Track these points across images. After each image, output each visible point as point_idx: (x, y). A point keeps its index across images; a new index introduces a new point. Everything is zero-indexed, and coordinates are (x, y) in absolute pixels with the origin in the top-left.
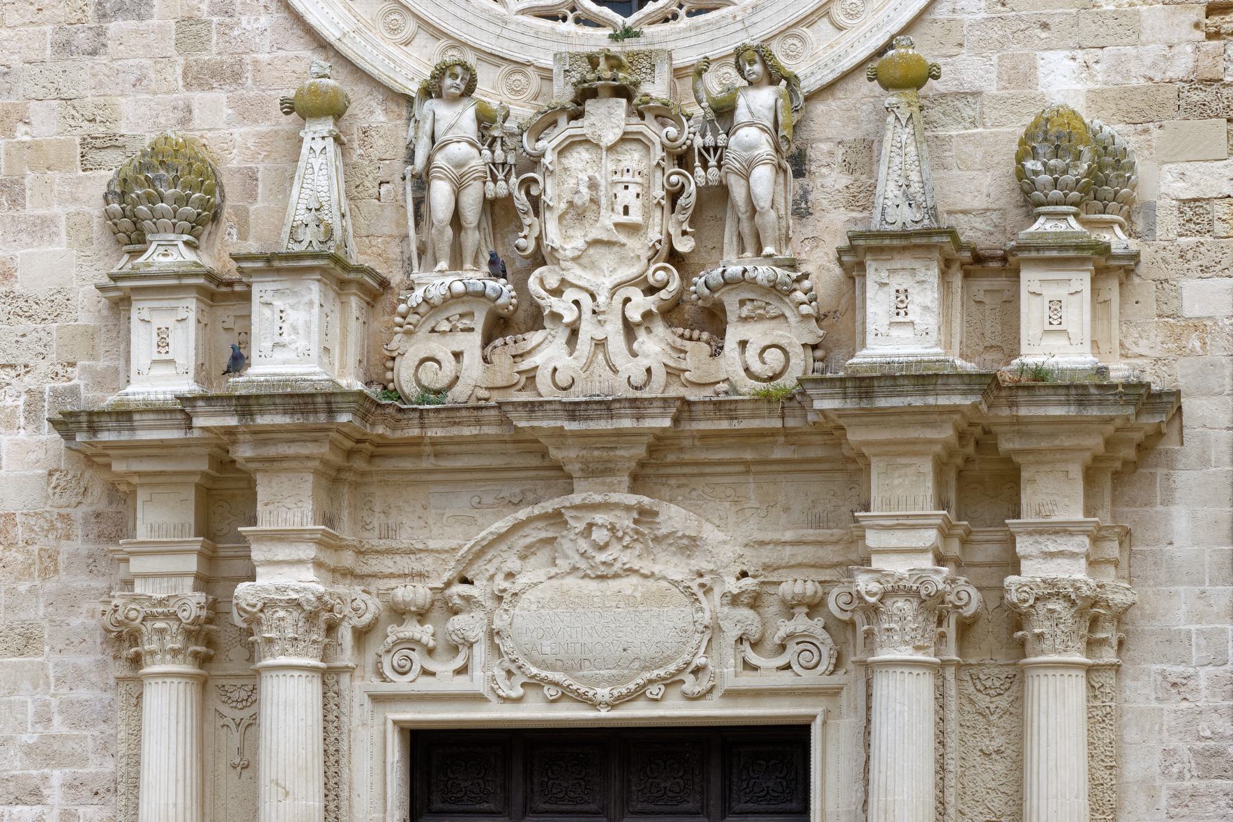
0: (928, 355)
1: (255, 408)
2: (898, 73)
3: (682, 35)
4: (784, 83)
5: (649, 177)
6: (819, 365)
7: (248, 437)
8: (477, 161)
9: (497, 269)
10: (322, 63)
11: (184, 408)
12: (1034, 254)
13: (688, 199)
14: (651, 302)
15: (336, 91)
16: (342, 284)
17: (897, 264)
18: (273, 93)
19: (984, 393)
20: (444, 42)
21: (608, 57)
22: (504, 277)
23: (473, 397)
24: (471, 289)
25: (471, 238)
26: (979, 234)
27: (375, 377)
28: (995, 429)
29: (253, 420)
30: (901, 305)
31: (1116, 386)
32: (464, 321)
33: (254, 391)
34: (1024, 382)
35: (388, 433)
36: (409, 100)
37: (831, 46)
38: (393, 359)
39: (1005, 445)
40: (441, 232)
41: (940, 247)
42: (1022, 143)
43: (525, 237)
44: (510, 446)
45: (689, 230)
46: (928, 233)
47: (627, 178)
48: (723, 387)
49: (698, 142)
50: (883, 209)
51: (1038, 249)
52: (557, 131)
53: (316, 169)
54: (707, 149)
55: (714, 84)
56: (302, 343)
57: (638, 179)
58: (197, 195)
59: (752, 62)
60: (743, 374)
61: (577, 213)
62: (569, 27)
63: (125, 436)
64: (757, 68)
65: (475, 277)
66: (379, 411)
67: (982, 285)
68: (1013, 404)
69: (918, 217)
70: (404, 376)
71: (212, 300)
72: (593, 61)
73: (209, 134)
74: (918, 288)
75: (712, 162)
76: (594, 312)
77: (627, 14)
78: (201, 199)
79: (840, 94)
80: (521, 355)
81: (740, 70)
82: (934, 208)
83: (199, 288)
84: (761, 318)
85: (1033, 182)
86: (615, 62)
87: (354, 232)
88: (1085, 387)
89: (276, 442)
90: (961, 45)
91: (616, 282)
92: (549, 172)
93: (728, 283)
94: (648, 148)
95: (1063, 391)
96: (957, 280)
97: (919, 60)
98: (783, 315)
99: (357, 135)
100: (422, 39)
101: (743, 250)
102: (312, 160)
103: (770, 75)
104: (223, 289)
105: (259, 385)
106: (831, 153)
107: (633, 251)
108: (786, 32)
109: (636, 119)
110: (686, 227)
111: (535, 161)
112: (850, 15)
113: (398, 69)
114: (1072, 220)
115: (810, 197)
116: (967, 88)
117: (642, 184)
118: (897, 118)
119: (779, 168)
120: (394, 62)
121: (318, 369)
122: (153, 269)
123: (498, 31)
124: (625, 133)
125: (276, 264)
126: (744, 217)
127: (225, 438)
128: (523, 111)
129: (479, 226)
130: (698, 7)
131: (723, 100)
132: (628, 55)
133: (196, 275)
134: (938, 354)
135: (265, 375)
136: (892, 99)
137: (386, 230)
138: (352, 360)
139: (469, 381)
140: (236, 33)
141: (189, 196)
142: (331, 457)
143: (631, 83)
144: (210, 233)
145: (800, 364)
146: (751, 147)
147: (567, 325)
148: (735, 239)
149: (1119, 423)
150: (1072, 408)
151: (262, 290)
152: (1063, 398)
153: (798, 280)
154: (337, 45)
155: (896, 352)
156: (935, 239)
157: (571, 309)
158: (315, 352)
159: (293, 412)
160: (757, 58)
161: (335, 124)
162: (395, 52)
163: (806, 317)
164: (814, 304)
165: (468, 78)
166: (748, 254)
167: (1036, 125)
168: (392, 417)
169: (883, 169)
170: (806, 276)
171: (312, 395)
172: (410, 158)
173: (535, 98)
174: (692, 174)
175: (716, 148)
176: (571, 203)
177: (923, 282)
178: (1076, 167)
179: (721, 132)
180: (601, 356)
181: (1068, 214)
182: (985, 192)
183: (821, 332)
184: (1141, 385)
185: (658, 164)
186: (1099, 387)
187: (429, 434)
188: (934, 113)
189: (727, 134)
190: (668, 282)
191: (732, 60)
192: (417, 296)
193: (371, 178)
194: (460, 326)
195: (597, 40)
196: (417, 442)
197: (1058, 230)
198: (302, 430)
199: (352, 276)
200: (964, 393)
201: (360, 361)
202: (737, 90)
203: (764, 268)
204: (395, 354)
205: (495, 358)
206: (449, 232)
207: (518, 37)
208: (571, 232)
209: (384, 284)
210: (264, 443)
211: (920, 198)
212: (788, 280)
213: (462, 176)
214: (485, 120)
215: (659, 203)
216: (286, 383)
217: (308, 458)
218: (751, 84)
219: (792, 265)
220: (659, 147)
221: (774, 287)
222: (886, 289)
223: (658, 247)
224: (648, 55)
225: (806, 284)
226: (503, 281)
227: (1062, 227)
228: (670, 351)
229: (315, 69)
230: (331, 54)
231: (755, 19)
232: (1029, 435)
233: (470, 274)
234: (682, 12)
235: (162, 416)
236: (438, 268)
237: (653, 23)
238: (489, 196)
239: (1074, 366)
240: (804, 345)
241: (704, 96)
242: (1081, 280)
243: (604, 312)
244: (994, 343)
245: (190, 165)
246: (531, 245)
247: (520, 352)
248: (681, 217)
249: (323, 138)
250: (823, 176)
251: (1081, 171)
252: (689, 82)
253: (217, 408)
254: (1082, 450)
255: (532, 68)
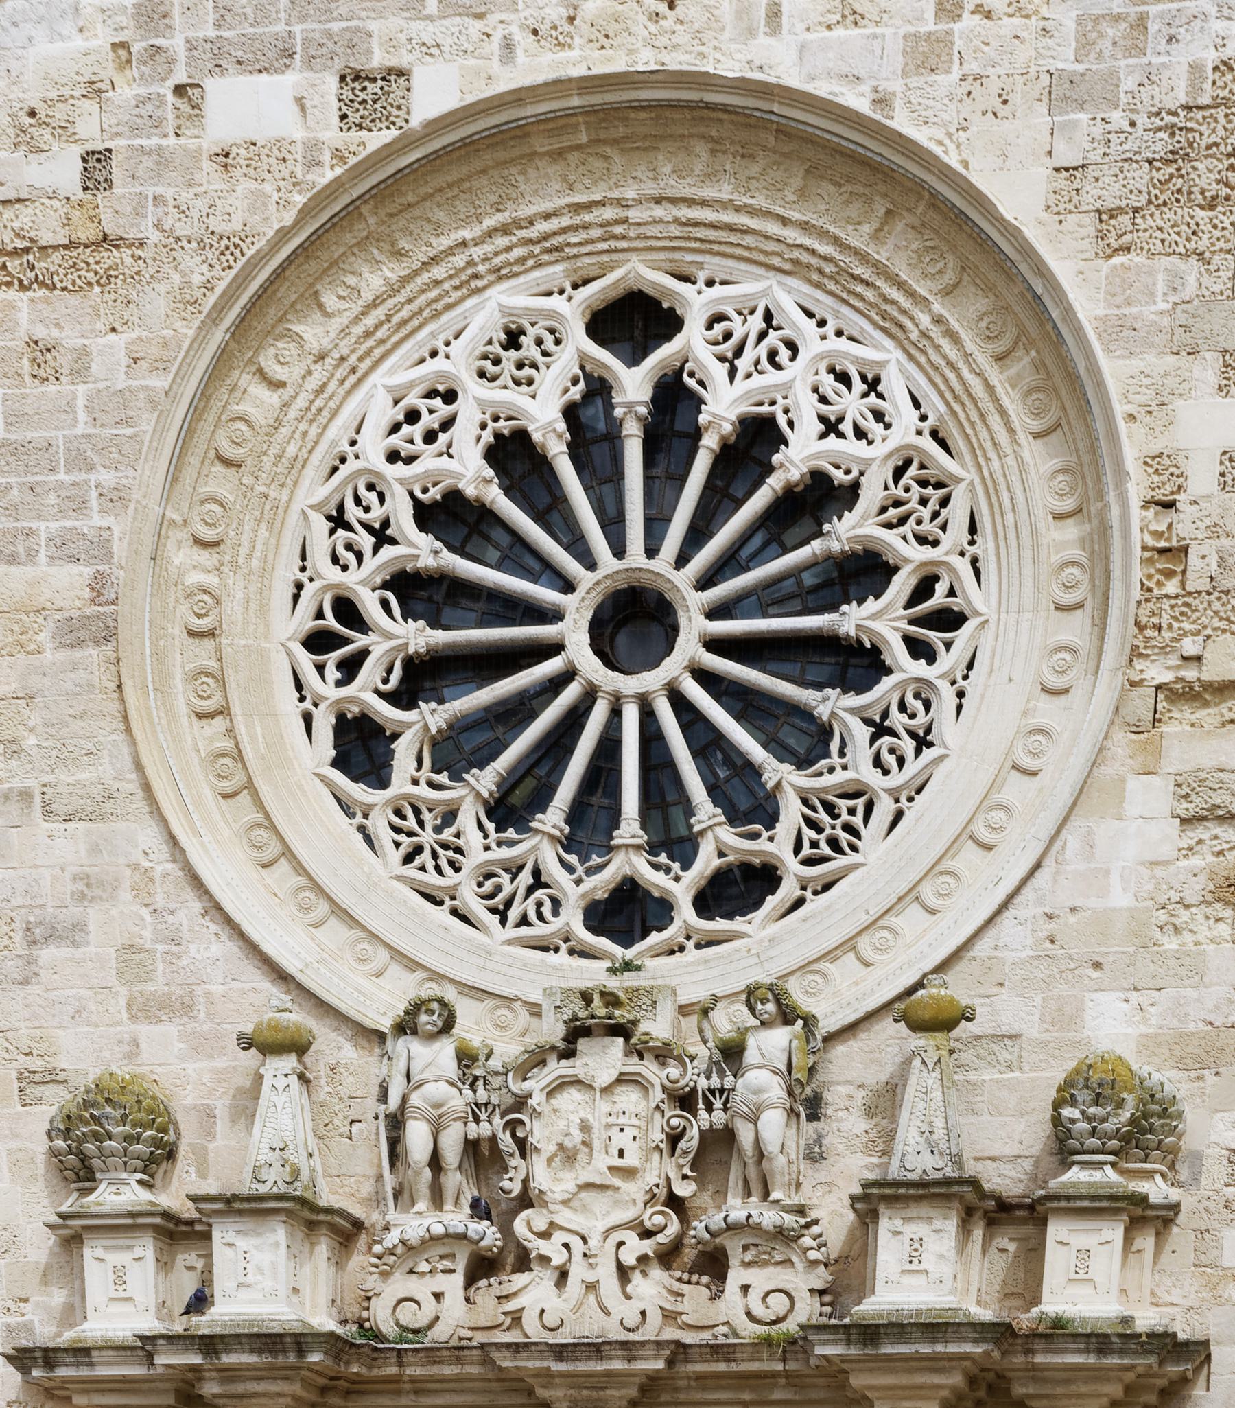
0: (941, 1302)
1: (220, 1347)
2: (927, 1015)
3: (690, 969)
4: (800, 1022)
5: (649, 1120)
6: (827, 1309)
7: (214, 1374)
8: (458, 1101)
9: (480, 1210)
10: (283, 996)
11: (147, 1345)
12: (1063, 1204)
13: (691, 1141)
14: (647, 1246)
15: (298, 1028)
16: (311, 1225)
17: (913, 1211)
18: (228, 1026)
19: (997, 1342)
20: (420, 975)
21: (603, 994)
22: (489, 1218)
23: (455, 1337)
24: (451, 1230)
25: (453, 1179)
26: (1008, 1181)
27: (349, 1315)
28: (1010, 1374)
29: (218, 1358)
30: (914, 1254)
31: (1140, 1335)
32: (445, 1262)
33: (218, 1331)
34: (1042, 1329)
35: (364, 1371)
36: (381, 1037)
37: (856, 983)
38: (369, 1299)
39: (1019, 1390)
40: (418, 1173)
41: (961, 1198)
42: (1060, 1090)
43: (511, 1179)
44: (494, 1384)
45: (690, 1174)
46: (948, 1182)
47: (622, 1120)
48: (725, 1329)
49: (703, 1083)
50: (903, 1155)
51: (1068, 1198)
52: (546, 1070)
53: (279, 1108)
54: (712, 1091)
55: (726, 1021)
56: (268, 1284)
57: (635, 1121)
58: (149, 1133)
59: (764, 1001)
60: (745, 1317)
61: (567, 1156)
62: (562, 958)
63: (84, 1372)
64: (771, 1007)
65: (457, 1218)
66: (353, 1351)
67: (1007, 1242)
68: (1029, 1351)
69: (940, 1164)
70: (382, 1317)
71: (171, 1239)
72: (586, 997)
73: (159, 1070)
74: (934, 1236)
75: (718, 1104)
76: (585, 1255)
77: (627, 944)
78: (153, 1138)
79: (863, 1036)
80: (507, 1297)
81: (752, 1009)
82: (959, 1155)
83: (155, 1228)
84: (765, 1263)
85: (1069, 1130)
86: (611, 1000)
87: (324, 1171)
88: (1106, 1336)
89: (243, 1379)
90: (1001, 985)
91: (609, 1226)
92: (536, 1114)
93: (730, 1228)
94: (646, 1089)
95: (1083, 1340)
96: (978, 1233)
97: (952, 1000)
98: (790, 1261)
99: (323, 1071)
100: (395, 970)
101: (749, 1195)
102: (274, 1098)
103: (785, 1014)
104: (183, 1228)
105: (224, 1324)
106: (850, 1097)
107: (628, 1194)
108: (806, 967)
109: (636, 1059)
110: (687, 1171)
111: (520, 1103)
112: (878, 950)
113: (368, 1003)
114: (1108, 1169)
115: (824, 1142)
116: (1005, 1030)
117: (639, 1127)
118: (924, 1062)
119: (792, 1113)
120: (364, 995)
121: (286, 1309)
122: (105, 1209)
123: (481, 962)
124: (621, 1074)
125: (237, 1205)
126: (750, 1161)
127: (190, 1375)
128: (508, 1050)
129: (460, 1167)
130: (708, 938)
131: (732, 1040)
132: (626, 991)
133: (152, 1215)
134: (950, 1302)
135: (231, 1314)
136: (919, 1041)
137: (359, 1170)
138: (323, 1299)
139: (451, 1321)
140: (185, 962)
141: (139, 1135)
142: (304, 1394)
143: (629, 1021)
144: (165, 1172)
145: (807, 1310)
146: (758, 1091)
147: (556, 1268)
148: (740, 1183)
149: (1140, 1370)
150: (1092, 1355)
151: (223, 1234)
152: (1082, 1346)
153: (807, 1226)
154: (300, 977)
155: (906, 1299)
156: (955, 1189)
157: (561, 1252)
158: (283, 1291)
159: (260, 1352)
160: (770, 997)
161: (300, 1061)
162: (367, 985)
163: (815, 1263)
164: (823, 1249)
165: (446, 1014)
166: (754, 1199)
167: (1077, 1071)
168: (368, 1356)
169: (904, 1115)
170: (816, 1222)
171: (281, 1336)
172: (383, 1097)
173: (524, 1034)
174: (695, 1117)
175: (722, 1091)
176: (561, 1146)
177: (941, 1230)
178: (1118, 1115)
179: (728, 1073)
180: (592, 1298)
181: (1105, 1163)
182: (1017, 1138)
183: (830, 1278)
184: (1165, 1335)
185: (658, 1107)
186: (1120, 1336)
187: (408, 1372)
188: (966, 1057)
189: (735, 1076)
190: (666, 1226)
191: (744, 997)
192: (392, 1238)
193: (340, 1116)
194: (440, 1267)
195: (593, 974)
196: (395, 1380)
197: (1092, 1179)
198: (271, 1368)
199: (322, 1217)
200: (976, 1341)
201: (333, 1301)
202: (747, 1029)
203: (771, 1213)
204: (370, 1294)
205: (479, 1299)
206: (427, 1173)
207: (504, 969)
208: (561, 1175)
209: (358, 1225)
210: (232, 1380)
211: (943, 1145)
212: (795, 1226)
213: (440, 1116)
214: (465, 1058)
215: (657, 1146)
216: (252, 1323)
217: (279, 1395)
218: (763, 1023)
219: (801, 1211)
220: (658, 1089)
221: (780, 1232)
222: (900, 1237)
223: (656, 1190)
224: (649, 991)
225: (815, 1230)
226: (487, 1223)
227: (1097, 1176)
228: (665, 1294)
229: (275, 1003)
230: (292, 986)
231: (772, 953)
232: (1044, 1381)
233: (451, 1216)
234: (690, 944)
235: (123, 1353)
236: (416, 1209)
237: (657, 955)
238: (470, 1137)
239: (1097, 1315)
240: (811, 1291)
241: (709, 1034)
242: (1114, 1231)
243: (596, 1256)
244: (1015, 1290)
245: (139, 1102)
246: (516, 1188)
247: (505, 1293)
248: (681, 1161)
249: (286, 1075)
250: (840, 1120)
251: (1123, 1120)
252: (694, 1019)
253: (180, 1347)
254: (1099, 1396)
255: (519, 1003)
